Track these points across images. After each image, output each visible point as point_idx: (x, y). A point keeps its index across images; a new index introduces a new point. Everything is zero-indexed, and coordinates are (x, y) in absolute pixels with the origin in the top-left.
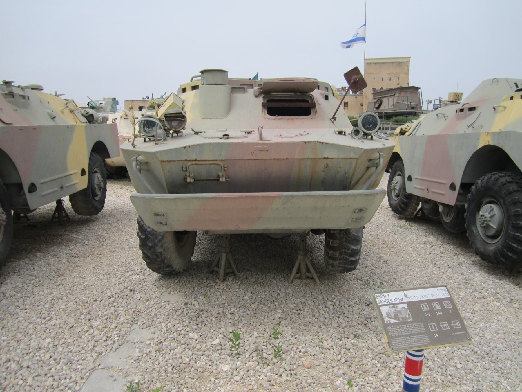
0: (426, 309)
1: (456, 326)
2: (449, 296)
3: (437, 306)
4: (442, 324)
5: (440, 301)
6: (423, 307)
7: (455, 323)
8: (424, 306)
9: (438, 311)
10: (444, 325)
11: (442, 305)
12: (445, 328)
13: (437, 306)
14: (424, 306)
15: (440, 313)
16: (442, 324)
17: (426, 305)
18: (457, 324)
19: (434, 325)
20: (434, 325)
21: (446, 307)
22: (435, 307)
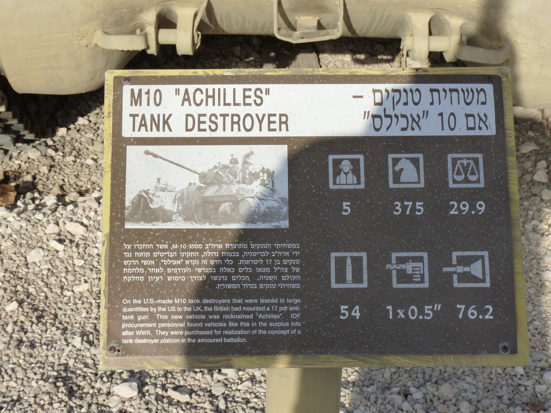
0: (346, 181)
1: (466, 277)
3: (409, 173)
4: (401, 260)
8: (346, 166)
9: (411, 194)
10: (409, 267)
12: (409, 279)
13: (409, 173)
14: (346, 166)
16: (401, 260)
17: (355, 163)
18: (476, 269)
19: (357, 261)
20: (357, 261)
21: (454, 180)
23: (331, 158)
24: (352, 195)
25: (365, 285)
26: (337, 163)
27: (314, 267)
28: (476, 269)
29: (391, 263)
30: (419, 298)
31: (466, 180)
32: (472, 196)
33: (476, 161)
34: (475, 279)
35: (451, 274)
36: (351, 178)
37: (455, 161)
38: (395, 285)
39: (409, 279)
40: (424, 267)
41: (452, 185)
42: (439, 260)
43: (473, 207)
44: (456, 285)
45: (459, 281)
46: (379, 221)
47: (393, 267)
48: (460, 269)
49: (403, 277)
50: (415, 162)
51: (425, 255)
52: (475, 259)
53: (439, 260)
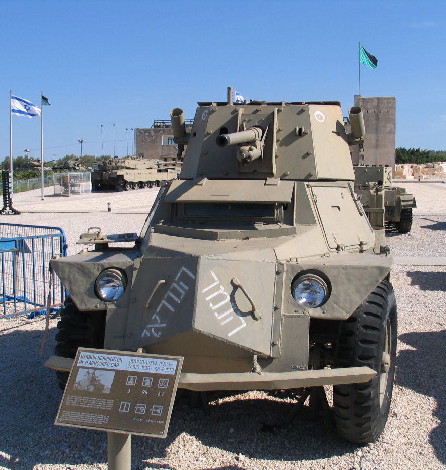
0: (131, 383)
1: (155, 412)
2: (173, 373)
4: (139, 406)
5: (156, 377)
6: (129, 381)
7: (156, 408)
8: (132, 379)
9: (146, 389)
10: (141, 408)
12: (140, 411)
13: (148, 383)
14: (132, 379)
16: (139, 406)
17: (134, 379)
18: (158, 411)
19: (127, 405)
20: (127, 405)
21: (160, 386)
22: (145, 383)
23: (128, 377)
24: (130, 387)
25: (128, 411)
26: (130, 378)
28: (158, 411)
29: (136, 406)
31: (163, 386)
32: (161, 390)
33: (167, 381)
34: (158, 413)
35: (151, 411)
36: (132, 383)
37: (161, 381)
38: (136, 412)
39: (140, 411)
41: (158, 387)
43: (161, 393)
44: (152, 414)
45: (153, 413)
46: (136, 395)
48: (154, 410)
49: (139, 410)
50: (150, 380)
51: (146, 405)
52: (159, 408)
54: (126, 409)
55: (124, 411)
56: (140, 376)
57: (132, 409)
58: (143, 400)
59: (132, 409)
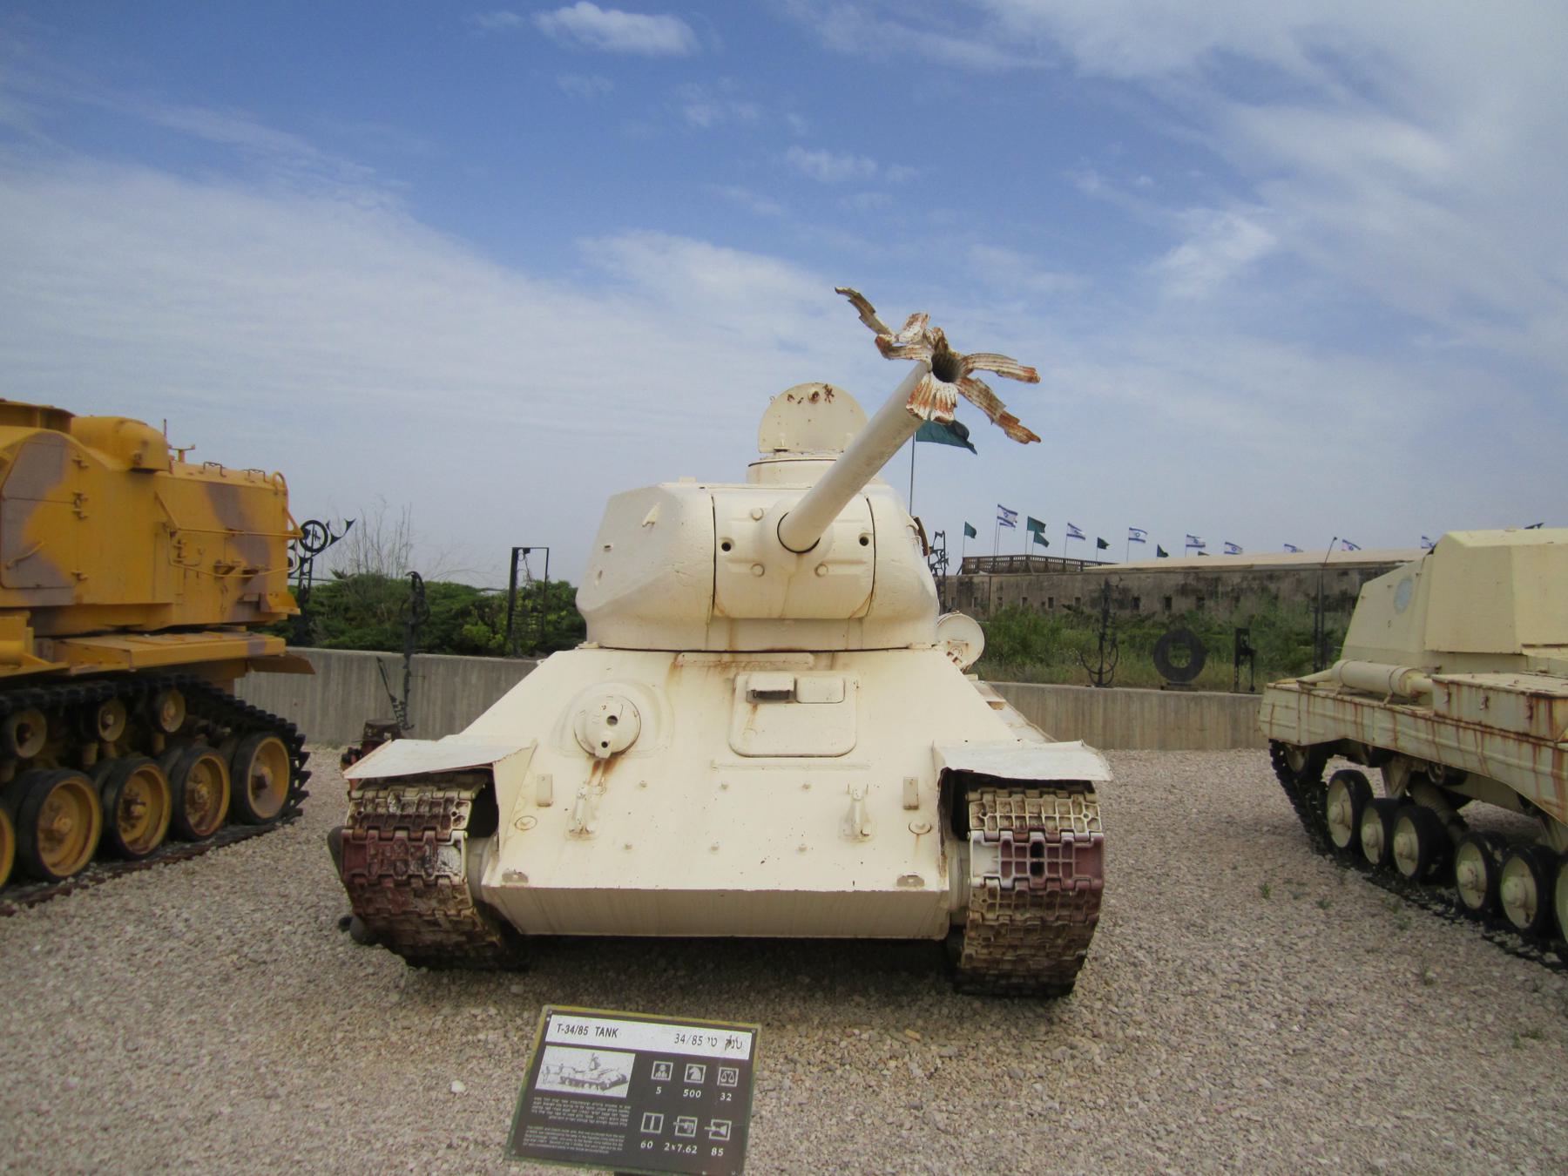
0: (661, 1076)
1: (716, 1134)
3: (696, 1074)
5: (711, 1064)
7: (718, 1125)
8: (663, 1068)
10: (686, 1125)
11: (711, 1076)
13: (696, 1074)
14: (663, 1068)
15: (698, 1094)
17: (668, 1067)
18: (723, 1130)
19: (658, 1120)
20: (658, 1120)
22: (689, 1076)
27: (635, 1118)
28: (723, 1130)
30: (686, 1142)
32: (727, 1090)
40: (694, 1126)
42: (703, 1122)
47: (677, 1124)
49: (682, 1130)
53: (703, 1122)
54: (656, 1127)
55: (651, 1130)
56: (681, 1061)
57: (669, 1127)
58: (689, 1107)
59: (669, 1127)
